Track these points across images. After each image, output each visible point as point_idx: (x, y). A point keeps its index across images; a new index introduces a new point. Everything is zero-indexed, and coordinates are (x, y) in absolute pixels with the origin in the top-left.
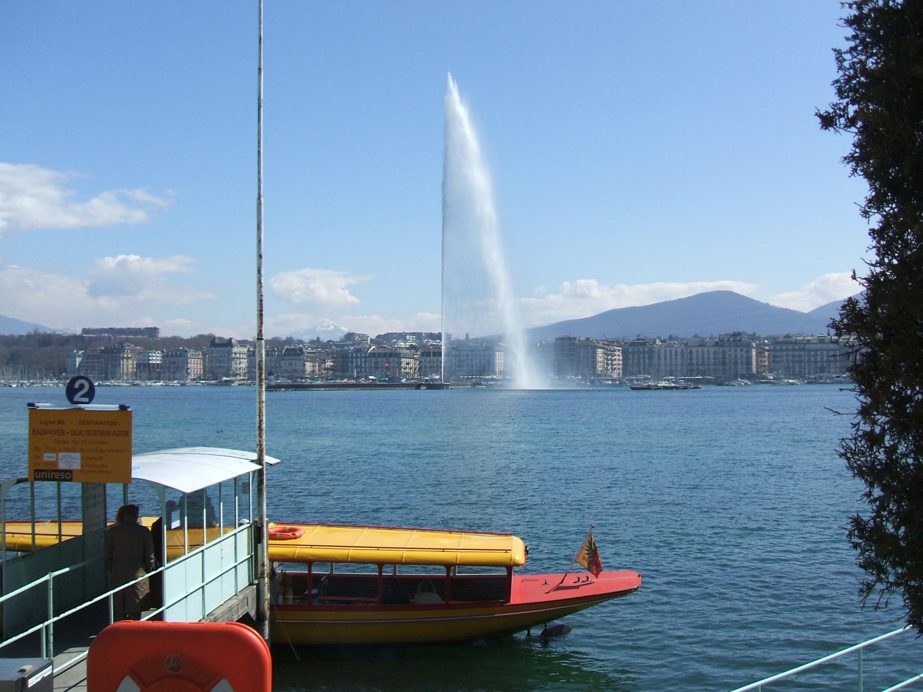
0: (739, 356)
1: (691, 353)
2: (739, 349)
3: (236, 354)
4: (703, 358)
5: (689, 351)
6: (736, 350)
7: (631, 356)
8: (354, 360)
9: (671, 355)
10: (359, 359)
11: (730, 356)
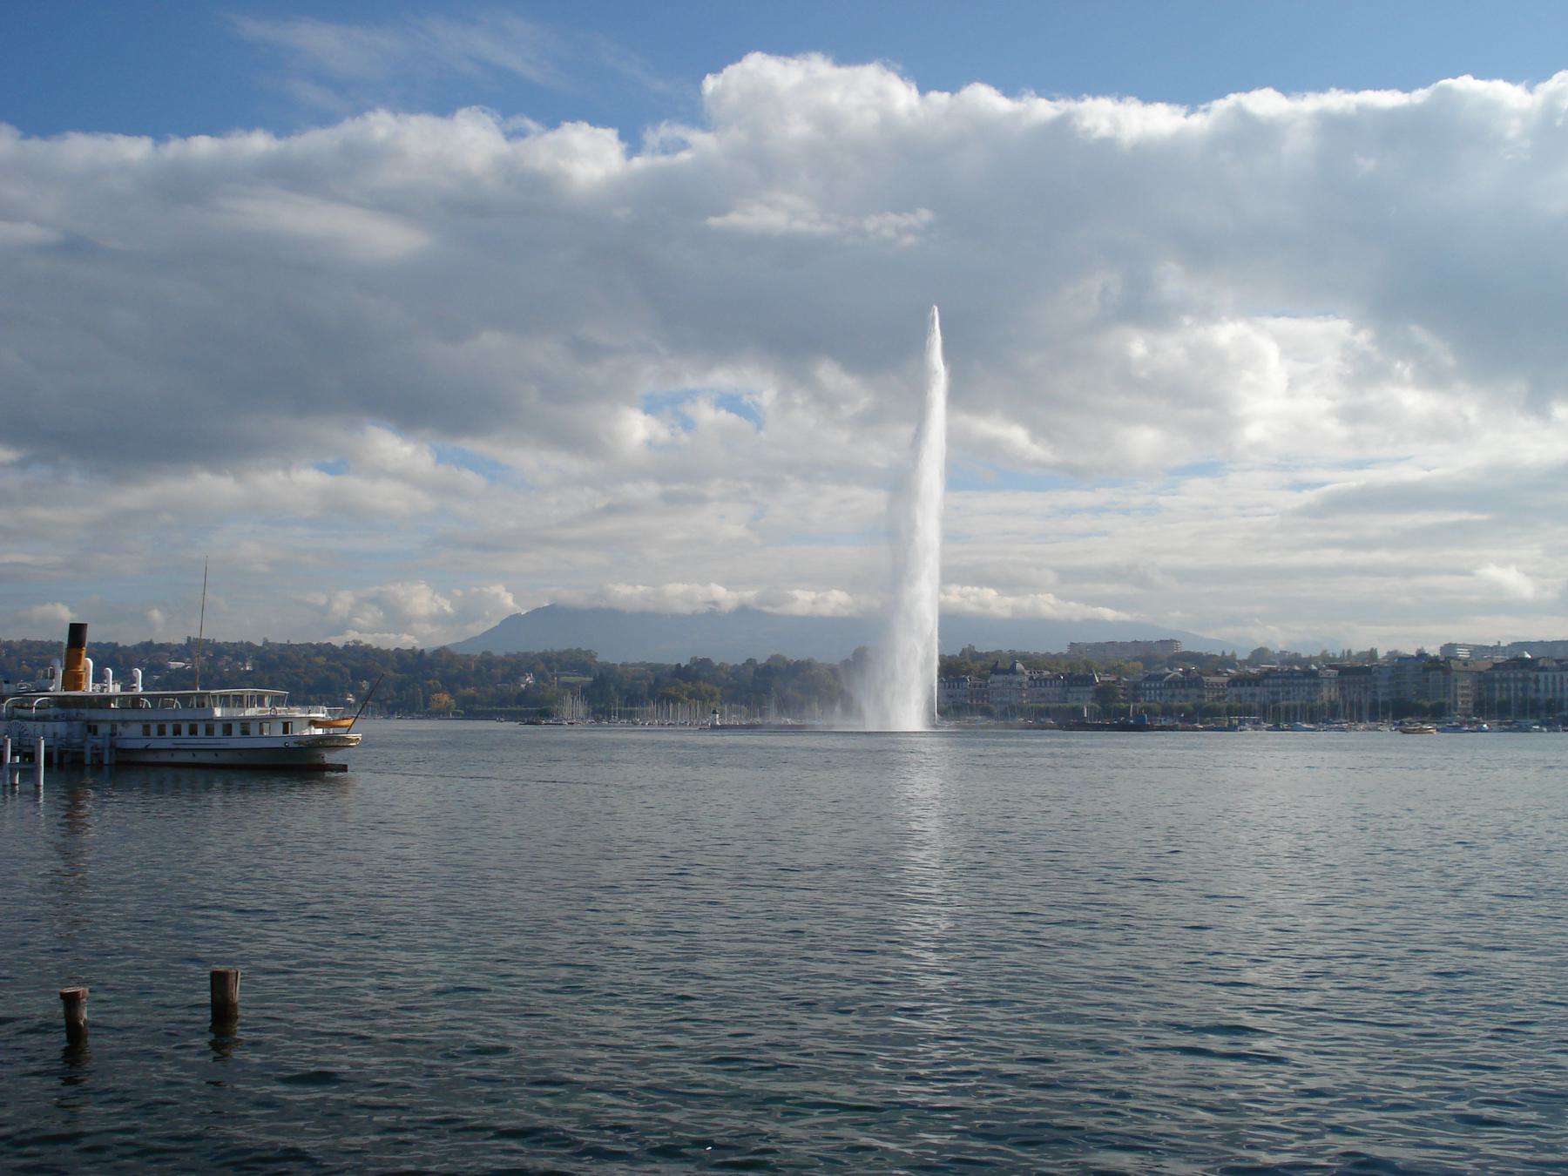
3: (1020, 684)
7: (1497, 686)
8: (1148, 692)
9: (1554, 683)
10: (1153, 692)
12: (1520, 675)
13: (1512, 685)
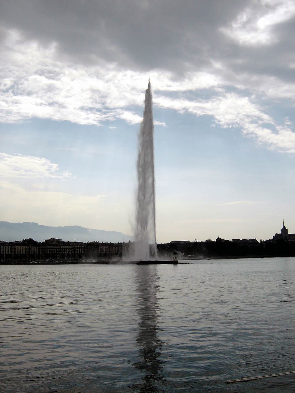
1: (15, 249)
2: (35, 248)
4: (20, 252)
5: (14, 247)
6: (34, 248)
9: (6, 249)
11: (32, 250)
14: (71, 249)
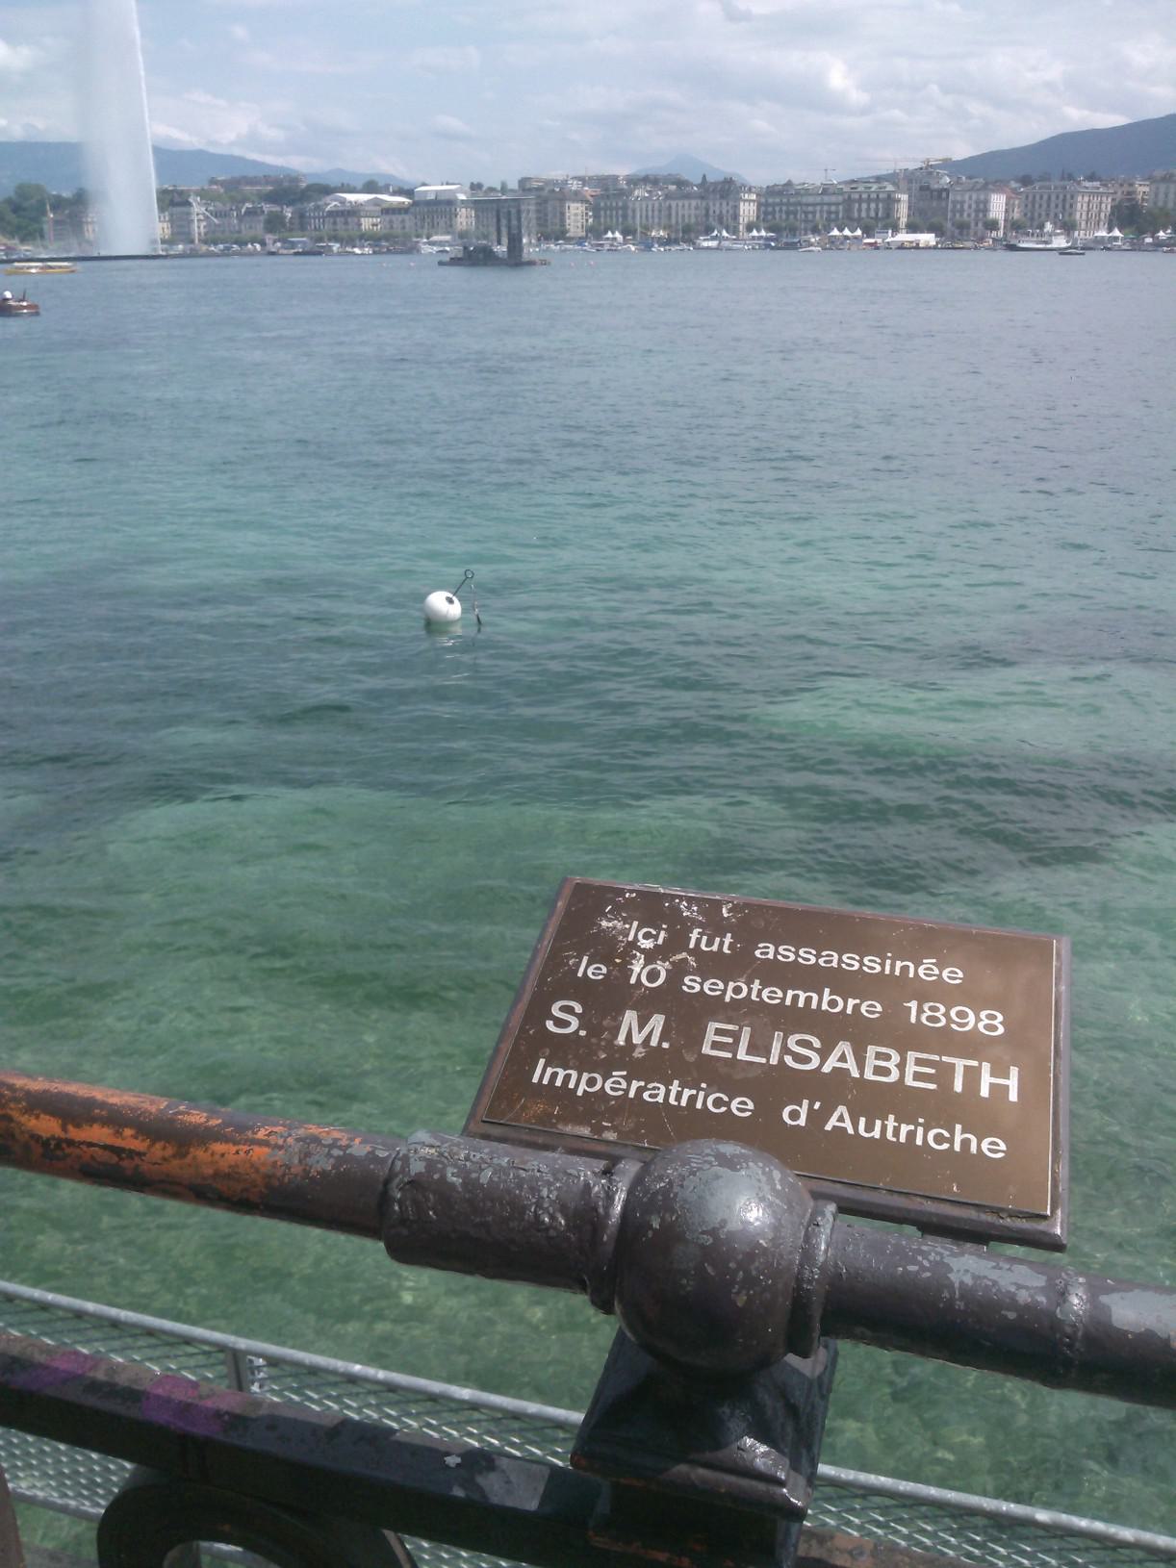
0: (724, 212)
1: (670, 207)
2: (724, 204)
4: (683, 216)
6: (721, 204)
7: (602, 213)
10: (317, 221)
11: (714, 212)
12: (620, 204)
13: (614, 213)
14: (837, 204)
